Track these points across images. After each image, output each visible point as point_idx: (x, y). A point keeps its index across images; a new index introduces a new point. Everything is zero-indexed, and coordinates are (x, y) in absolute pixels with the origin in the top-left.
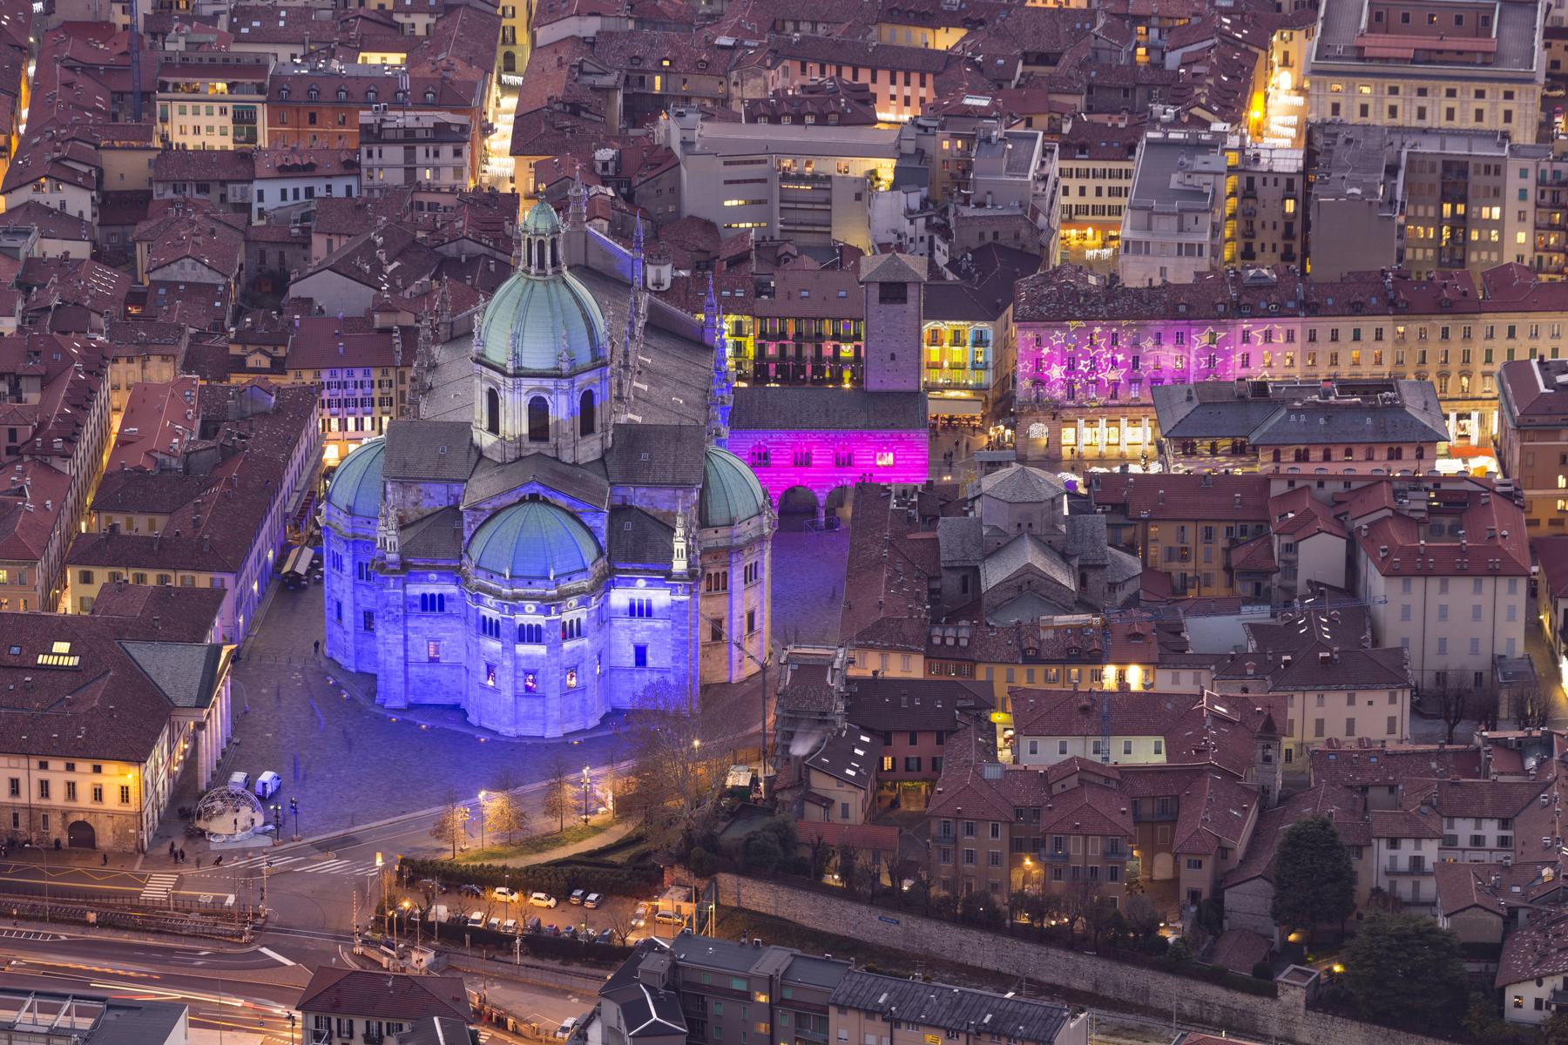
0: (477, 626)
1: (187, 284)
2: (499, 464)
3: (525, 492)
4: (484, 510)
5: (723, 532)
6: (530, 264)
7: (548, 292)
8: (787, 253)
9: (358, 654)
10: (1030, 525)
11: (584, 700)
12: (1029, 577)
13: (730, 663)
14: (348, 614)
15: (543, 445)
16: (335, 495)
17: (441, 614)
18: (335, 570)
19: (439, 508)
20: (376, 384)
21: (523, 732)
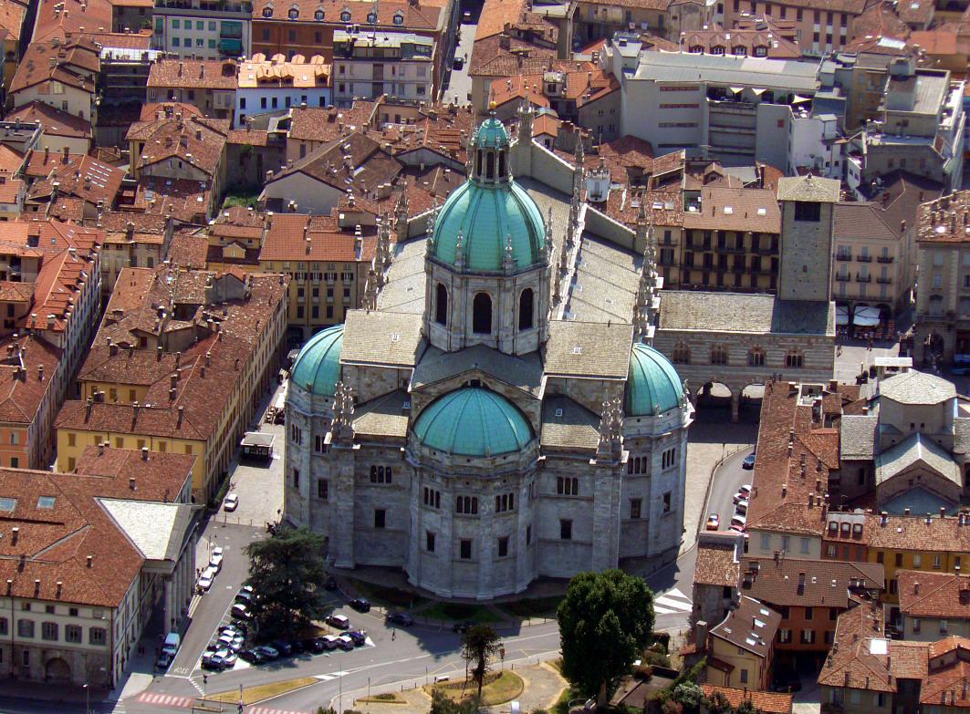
0: (420, 497)
1: (173, 180)
2: (445, 353)
3: (468, 378)
4: (429, 394)
5: (645, 421)
6: (479, 173)
7: (495, 199)
8: (714, 172)
9: (312, 518)
10: (923, 425)
11: (514, 568)
12: (919, 472)
13: (647, 539)
14: (304, 482)
15: (485, 337)
16: (297, 375)
17: (388, 485)
18: (294, 442)
19: (390, 390)
20: (339, 277)
21: (457, 594)
